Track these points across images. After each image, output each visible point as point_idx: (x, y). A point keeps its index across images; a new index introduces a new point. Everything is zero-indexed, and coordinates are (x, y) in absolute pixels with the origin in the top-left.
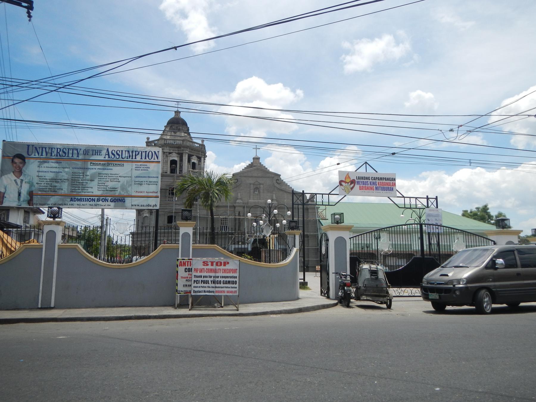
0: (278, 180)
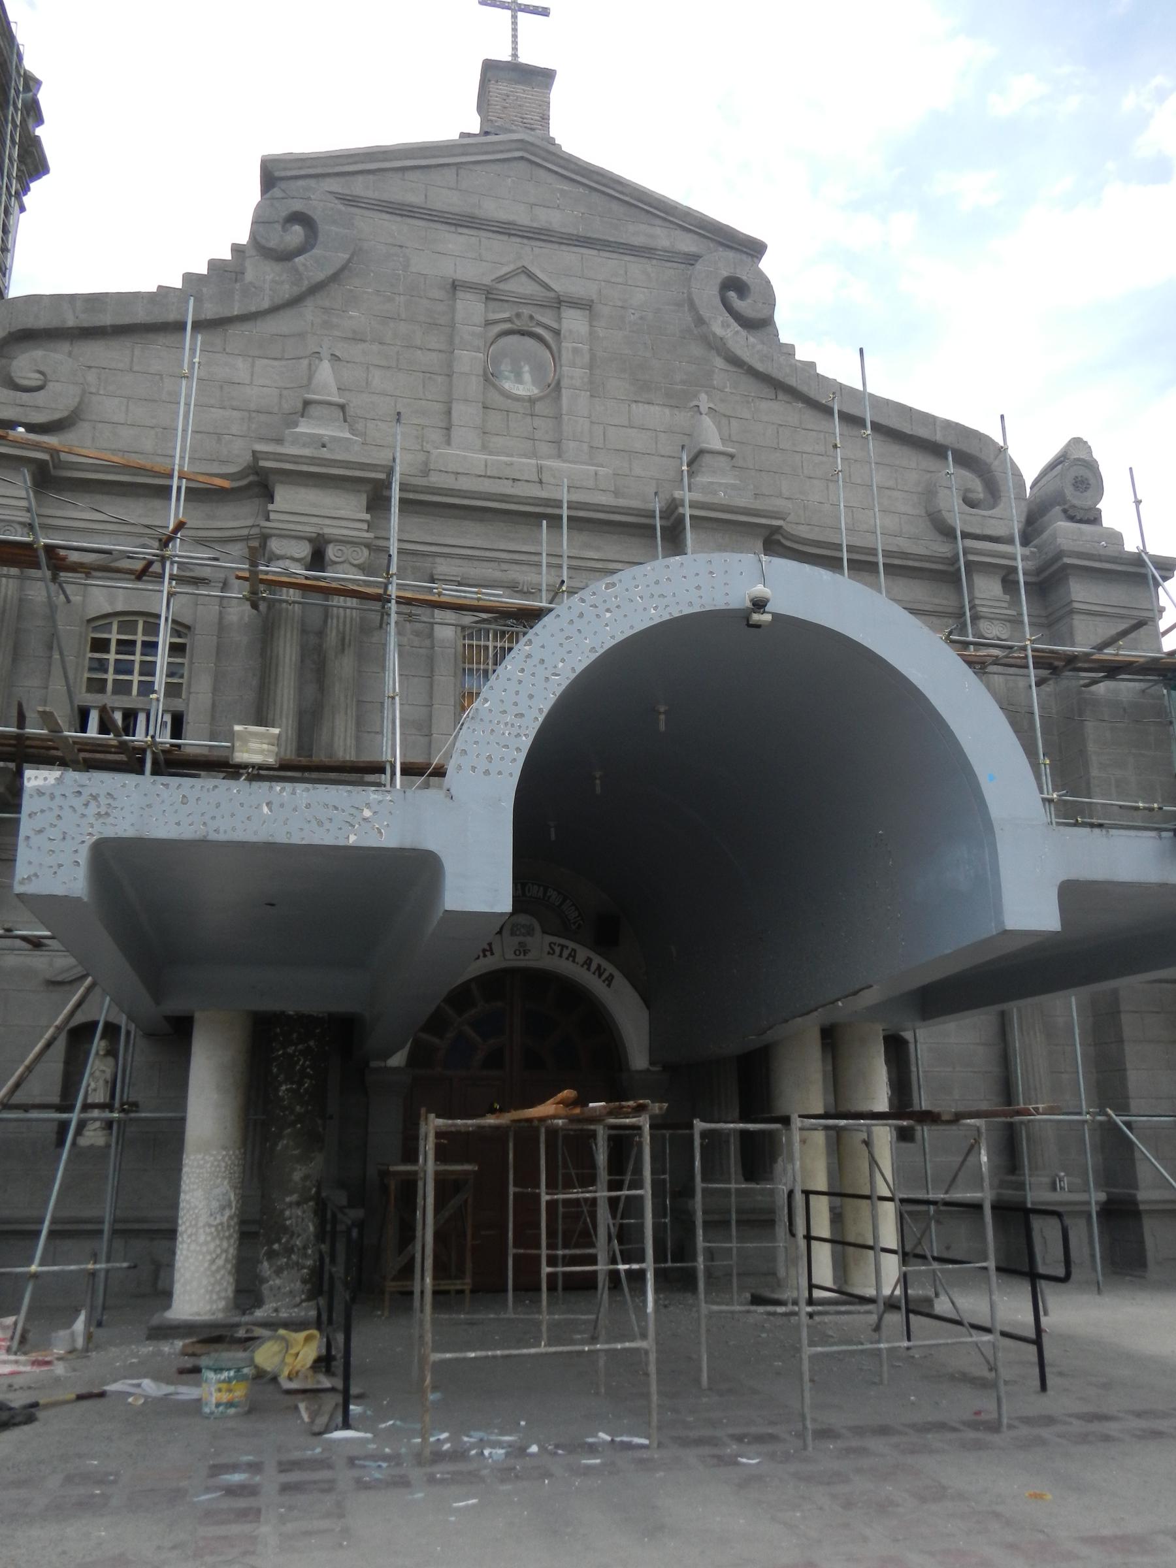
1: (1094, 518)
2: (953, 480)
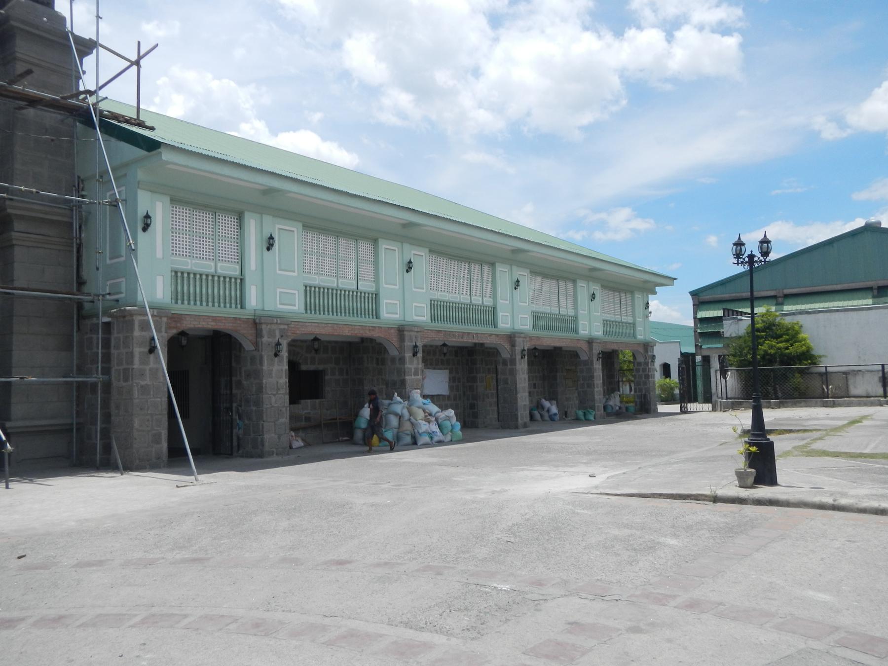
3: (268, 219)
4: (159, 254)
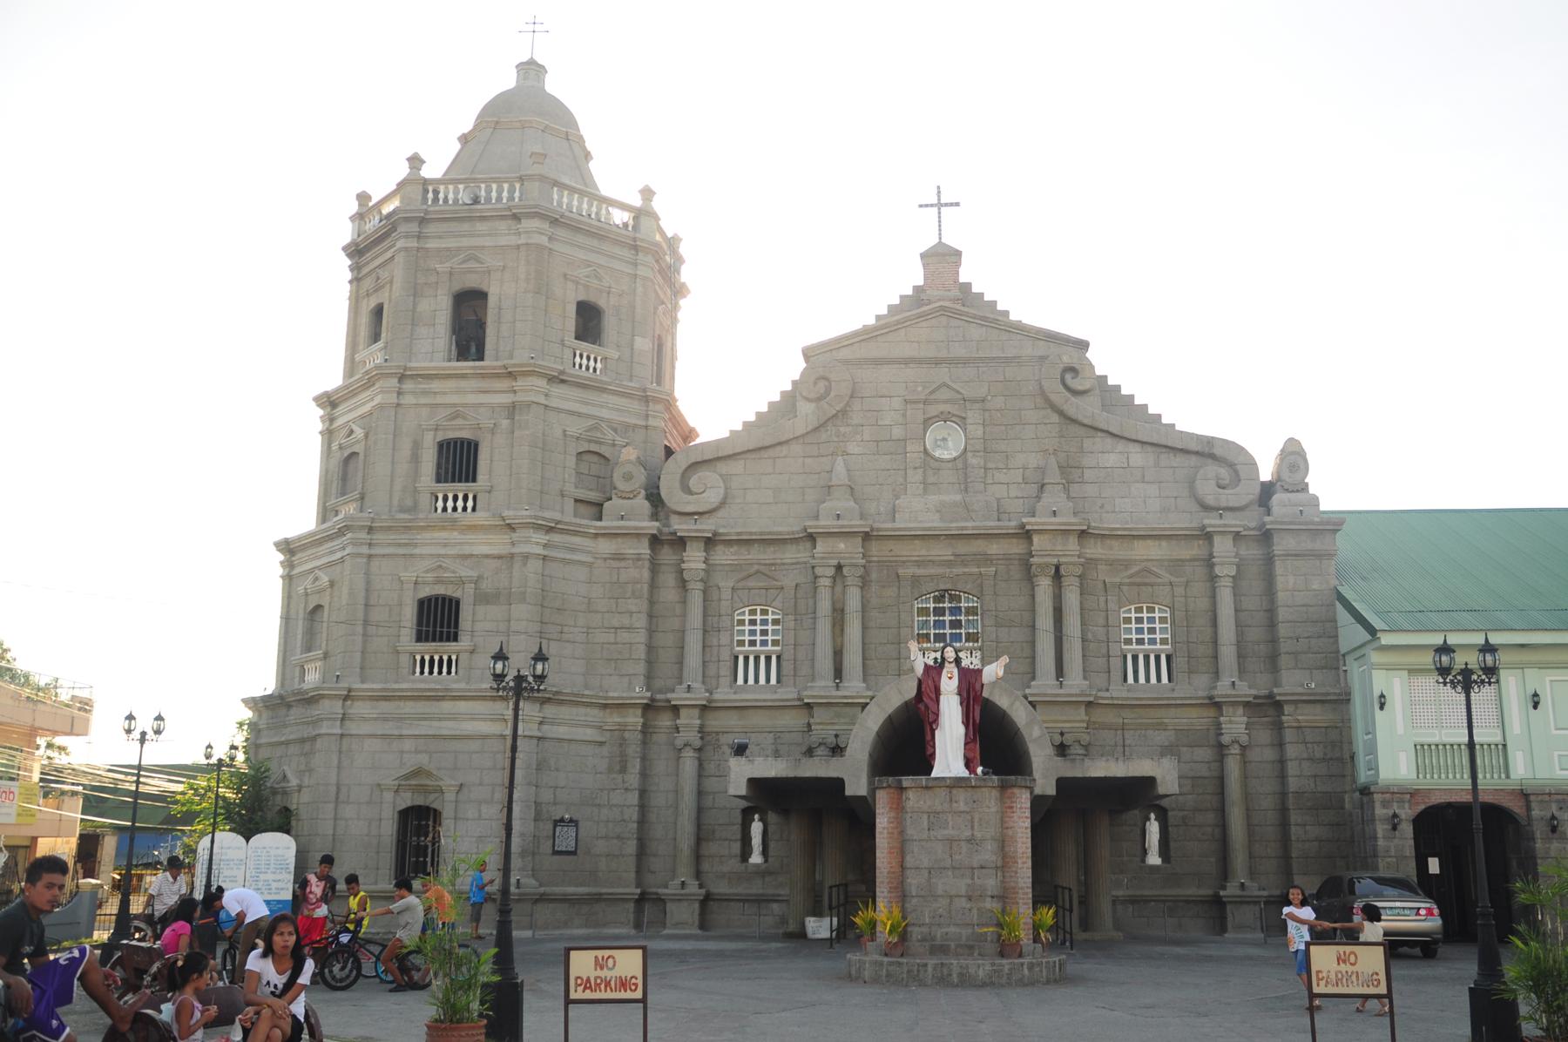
0: (1072, 370)
1: (1305, 488)
2: (1211, 469)
3: (1530, 673)
4: (1400, 731)
